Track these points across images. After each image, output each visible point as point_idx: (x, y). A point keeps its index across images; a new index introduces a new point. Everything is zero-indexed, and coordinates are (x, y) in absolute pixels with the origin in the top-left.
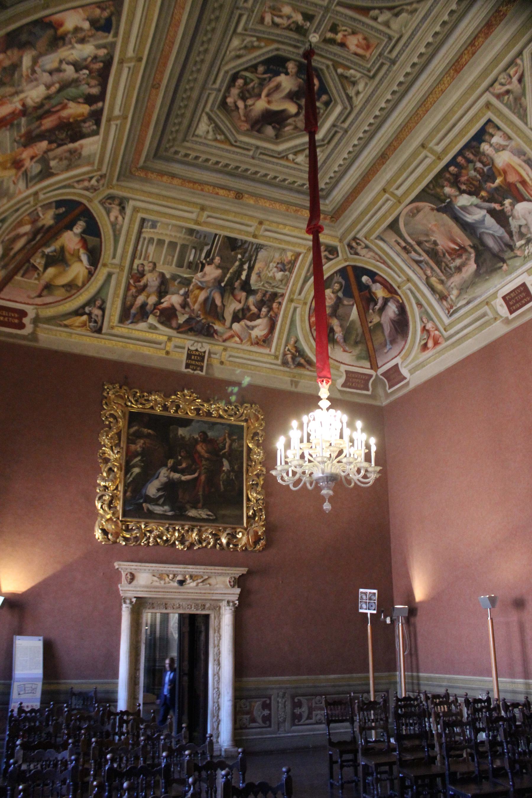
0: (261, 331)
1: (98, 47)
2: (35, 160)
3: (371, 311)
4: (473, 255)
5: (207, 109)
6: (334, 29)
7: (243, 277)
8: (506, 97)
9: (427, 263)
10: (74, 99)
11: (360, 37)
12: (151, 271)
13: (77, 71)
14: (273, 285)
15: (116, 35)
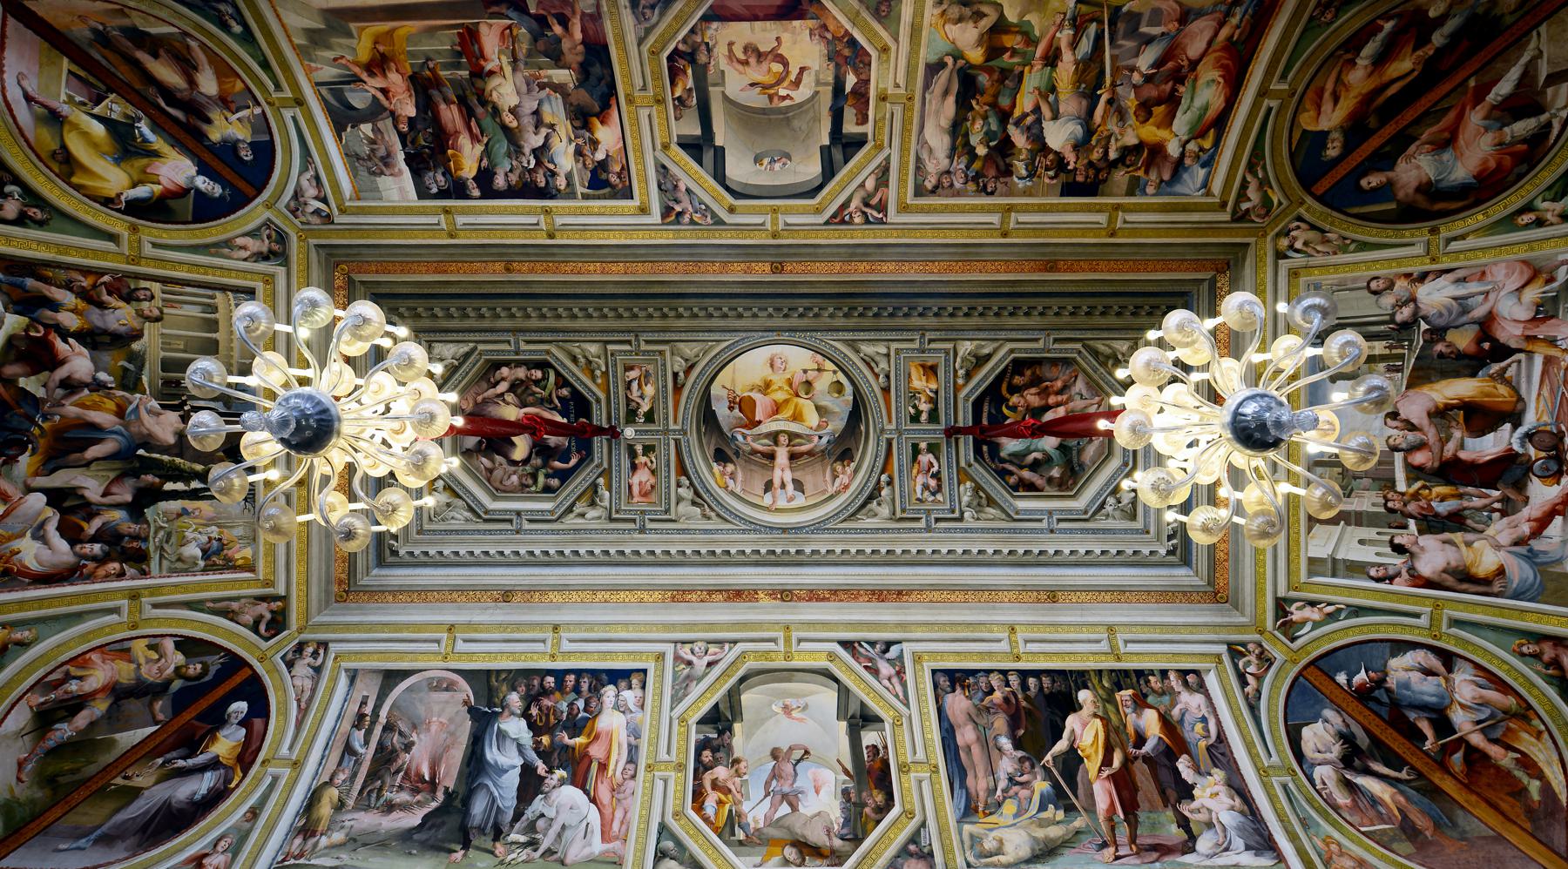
0: (36, 557)
1: (569, 176)
2: (380, 96)
3: (160, 761)
4: (434, 805)
5: (481, 347)
6: (648, 449)
7: (169, 486)
9: (358, 763)
10: (487, 152)
11: (653, 481)
12: (140, 314)
13: (534, 151)
14: (166, 547)
15: (585, 197)
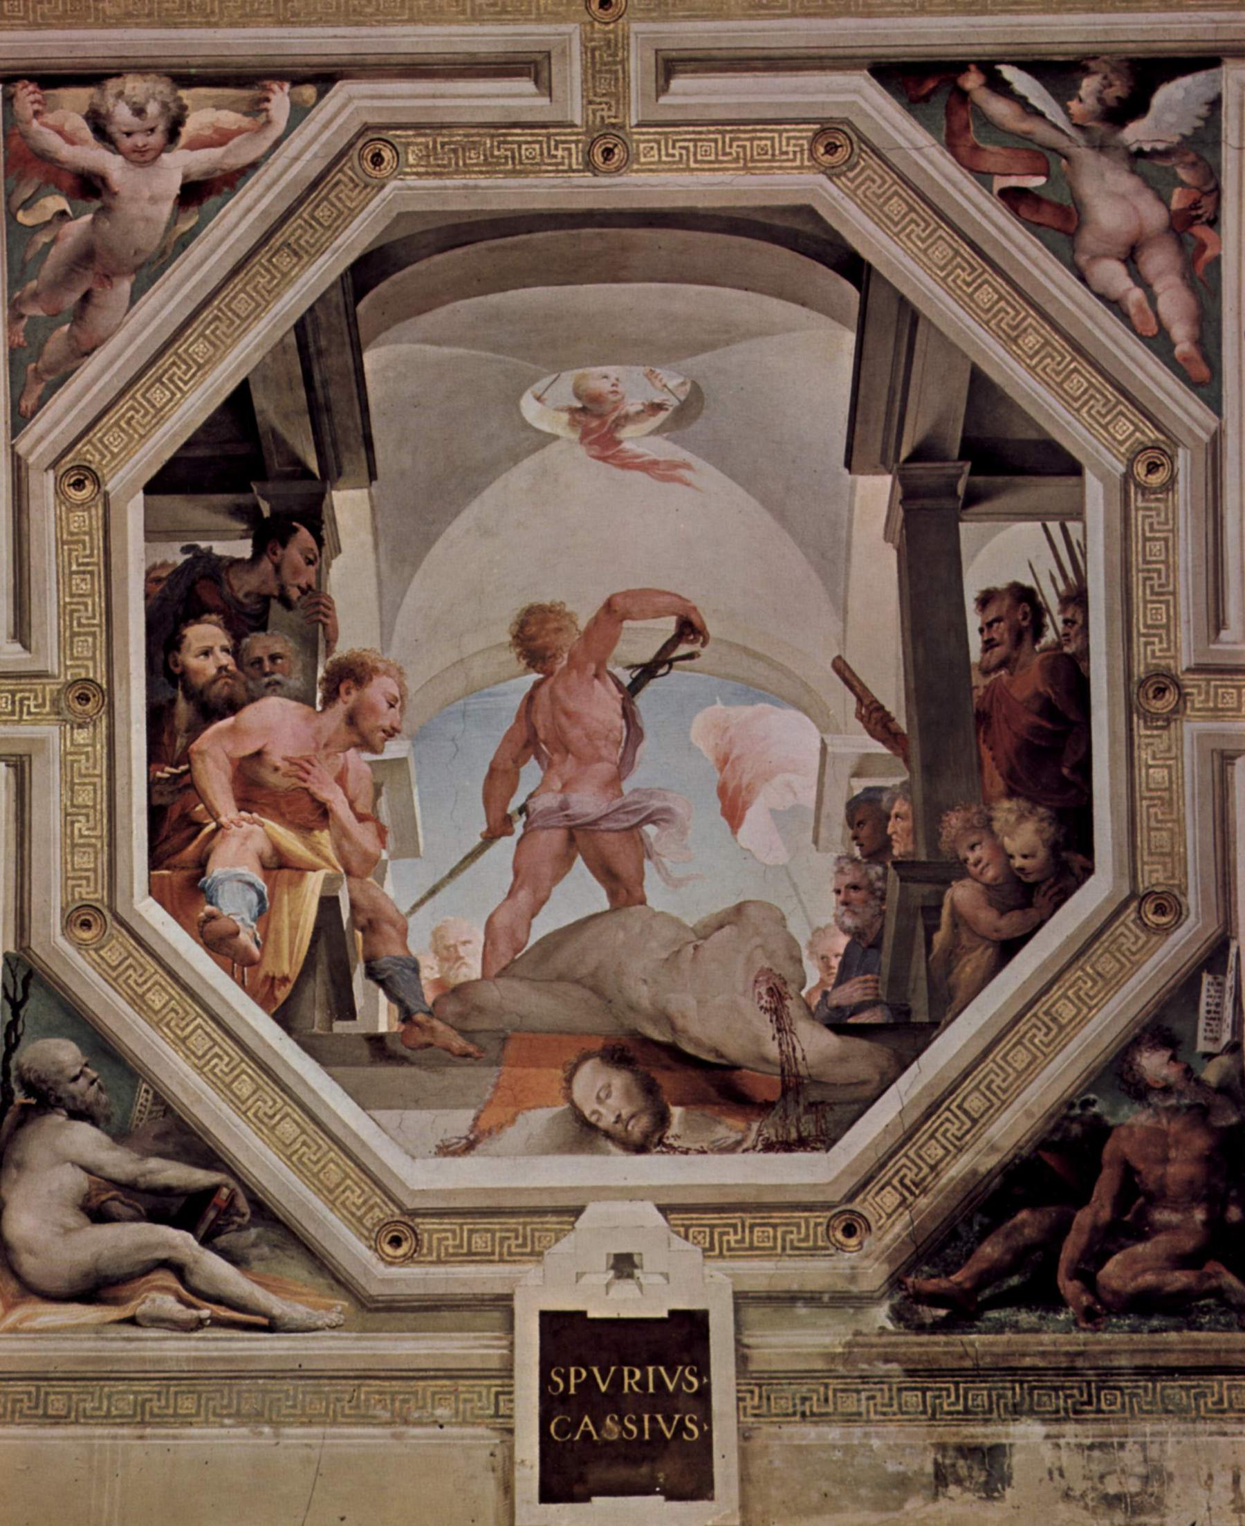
8: (56, 203)
